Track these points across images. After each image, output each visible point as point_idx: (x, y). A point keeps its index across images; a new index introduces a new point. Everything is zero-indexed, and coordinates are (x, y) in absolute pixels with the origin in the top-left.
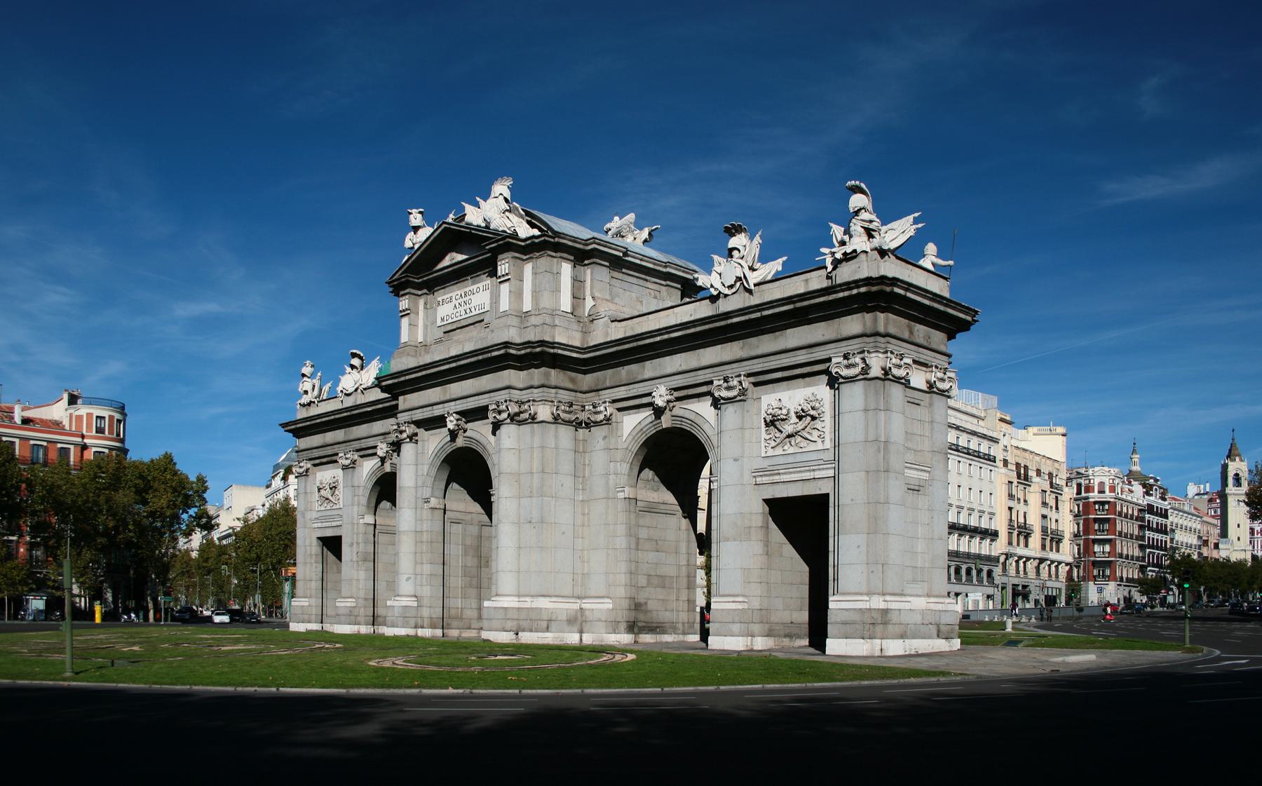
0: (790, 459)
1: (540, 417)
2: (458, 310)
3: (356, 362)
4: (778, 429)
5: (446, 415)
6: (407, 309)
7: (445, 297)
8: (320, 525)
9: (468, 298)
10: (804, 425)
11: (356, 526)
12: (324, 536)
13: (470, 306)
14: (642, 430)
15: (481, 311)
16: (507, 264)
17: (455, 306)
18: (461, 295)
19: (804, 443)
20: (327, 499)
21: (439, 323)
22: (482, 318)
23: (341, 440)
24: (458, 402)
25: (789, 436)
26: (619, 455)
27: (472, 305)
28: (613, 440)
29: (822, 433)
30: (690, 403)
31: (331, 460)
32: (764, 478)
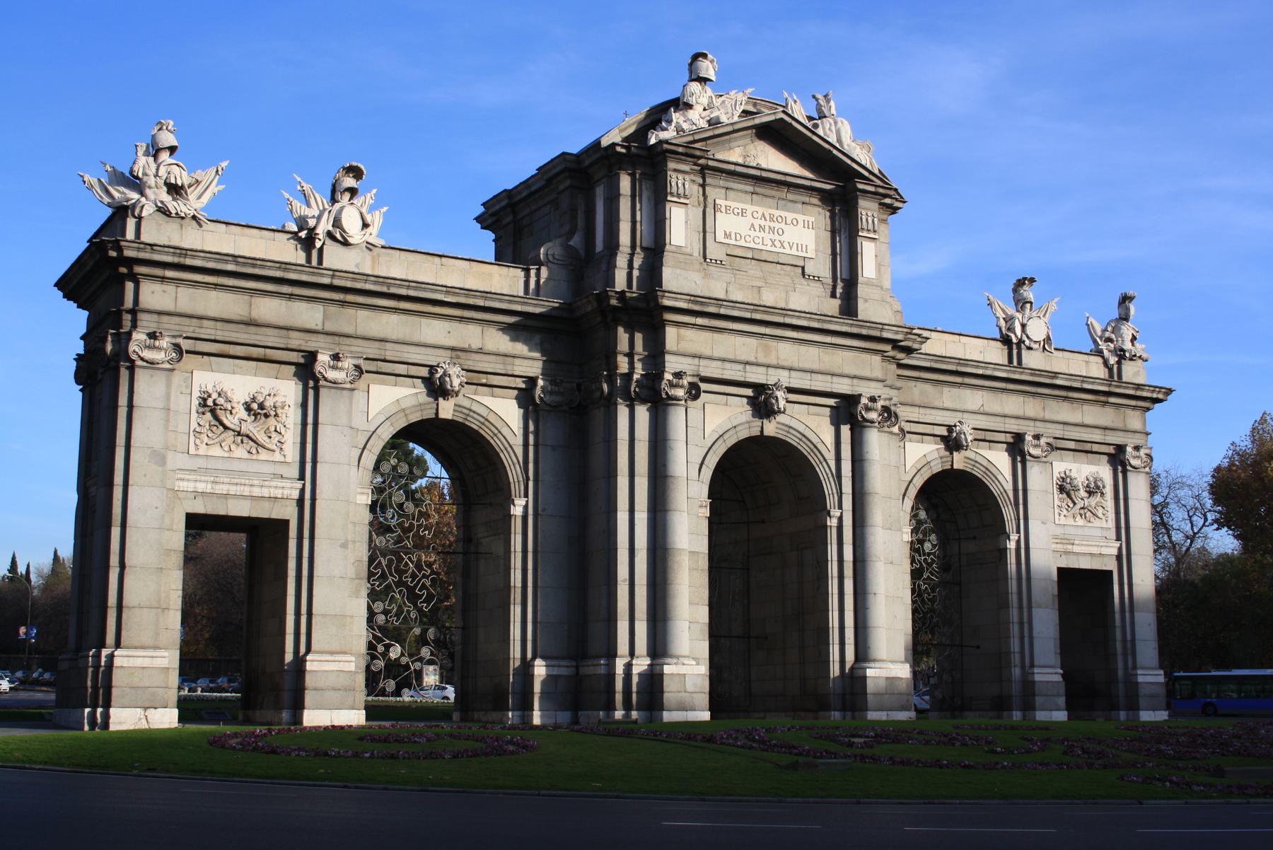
0: (1079, 532)
2: (757, 234)
3: (350, 182)
4: (1071, 499)
7: (733, 204)
8: (201, 487)
9: (777, 225)
12: (222, 512)
13: (782, 238)
15: (800, 254)
19: (1092, 519)
20: (248, 436)
22: (802, 264)
23: (311, 326)
24: (793, 374)
25: (1083, 508)
30: (981, 448)
32: (1059, 546)
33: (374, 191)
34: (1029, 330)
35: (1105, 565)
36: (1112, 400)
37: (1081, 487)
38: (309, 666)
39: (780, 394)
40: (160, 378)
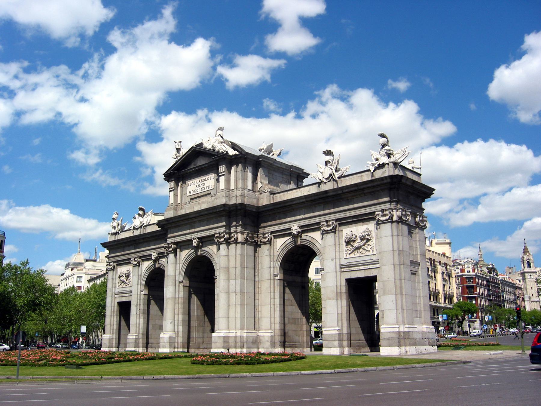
0: (358, 259)
1: (239, 240)
2: (198, 188)
3: (141, 212)
5: (193, 239)
6: (173, 188)
7: (191, 182)
9: (203, 182)
10: (363, 243)
11: (139, 296)
12: (121, 301)
13: (204, 186)
14: (286, 246)
15: (209, 189)
16: (224, 167)
17: (197, 186)
18: (199, 181)
19: (364, 252)
21: (188, 194)
26: (275, 259)
27: (205, 186)
28: (272, 251)
29: (372, 247)
31: (127, 262)
32: (346, 269)
33: (152, 210)
34: (323, 173)
35: (372, 273)
36: (366, 191)
37: (358, 237)
38: (128, 337)
39: (194, 241)
40: (112, 271)
